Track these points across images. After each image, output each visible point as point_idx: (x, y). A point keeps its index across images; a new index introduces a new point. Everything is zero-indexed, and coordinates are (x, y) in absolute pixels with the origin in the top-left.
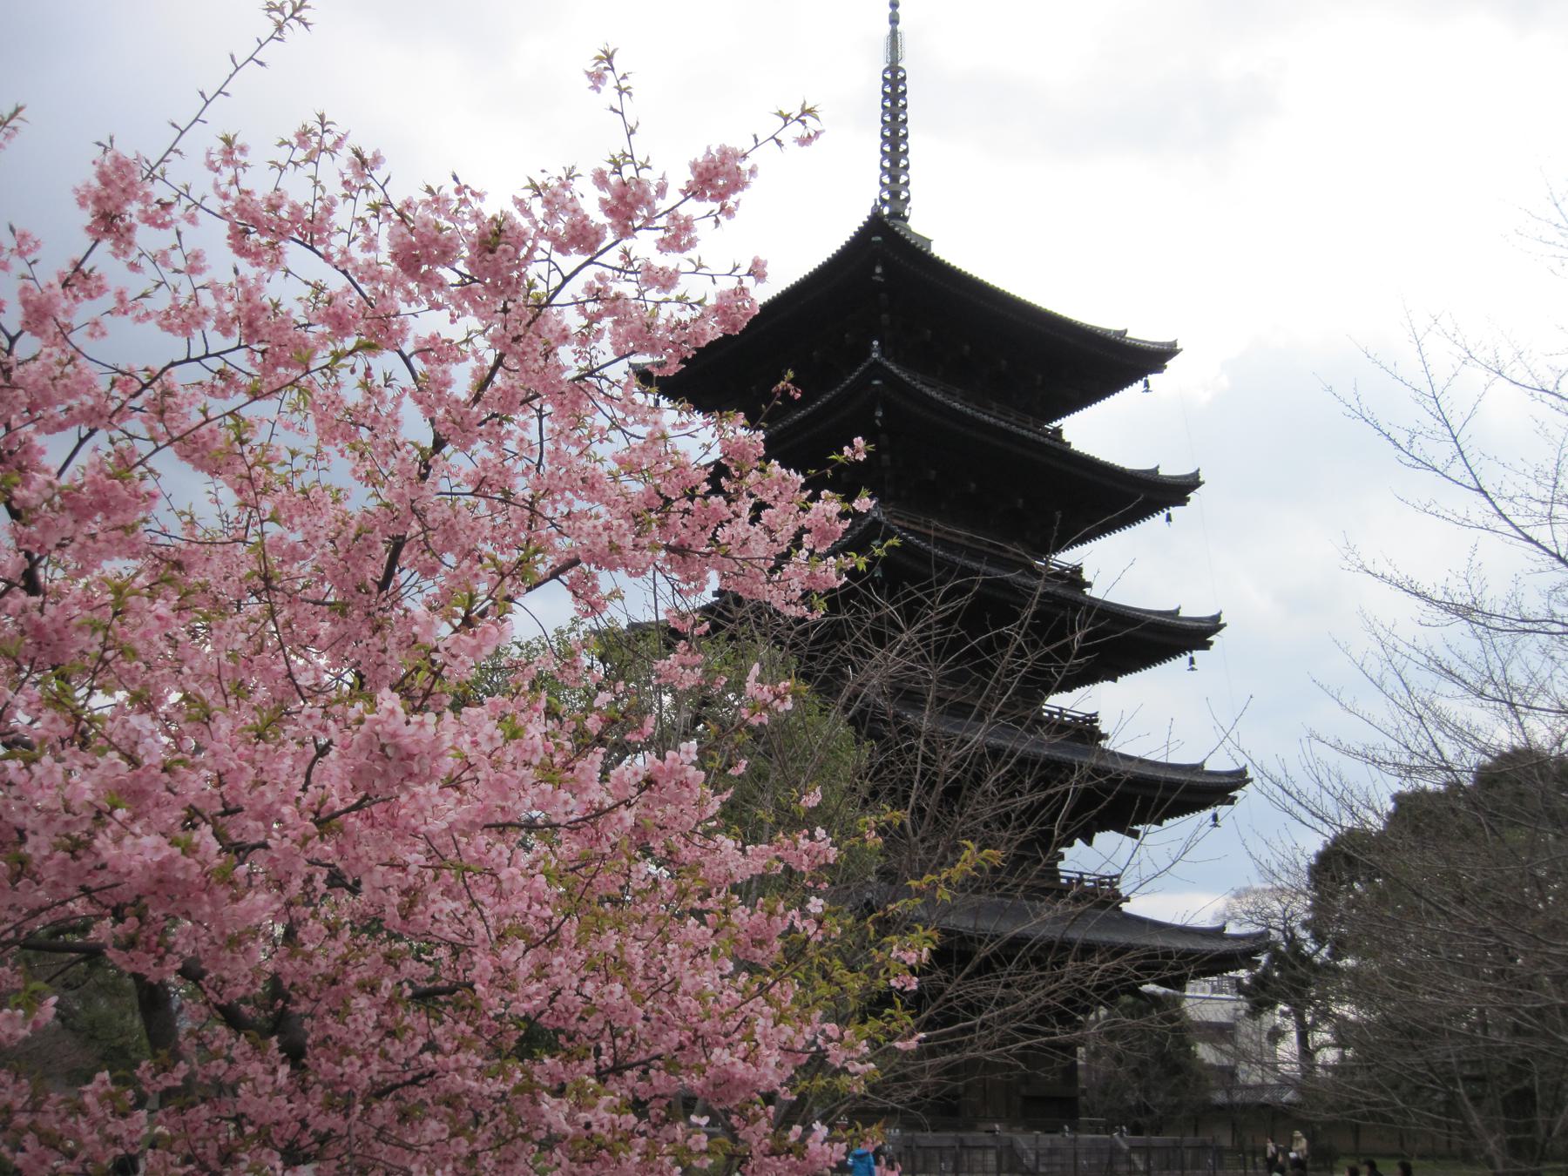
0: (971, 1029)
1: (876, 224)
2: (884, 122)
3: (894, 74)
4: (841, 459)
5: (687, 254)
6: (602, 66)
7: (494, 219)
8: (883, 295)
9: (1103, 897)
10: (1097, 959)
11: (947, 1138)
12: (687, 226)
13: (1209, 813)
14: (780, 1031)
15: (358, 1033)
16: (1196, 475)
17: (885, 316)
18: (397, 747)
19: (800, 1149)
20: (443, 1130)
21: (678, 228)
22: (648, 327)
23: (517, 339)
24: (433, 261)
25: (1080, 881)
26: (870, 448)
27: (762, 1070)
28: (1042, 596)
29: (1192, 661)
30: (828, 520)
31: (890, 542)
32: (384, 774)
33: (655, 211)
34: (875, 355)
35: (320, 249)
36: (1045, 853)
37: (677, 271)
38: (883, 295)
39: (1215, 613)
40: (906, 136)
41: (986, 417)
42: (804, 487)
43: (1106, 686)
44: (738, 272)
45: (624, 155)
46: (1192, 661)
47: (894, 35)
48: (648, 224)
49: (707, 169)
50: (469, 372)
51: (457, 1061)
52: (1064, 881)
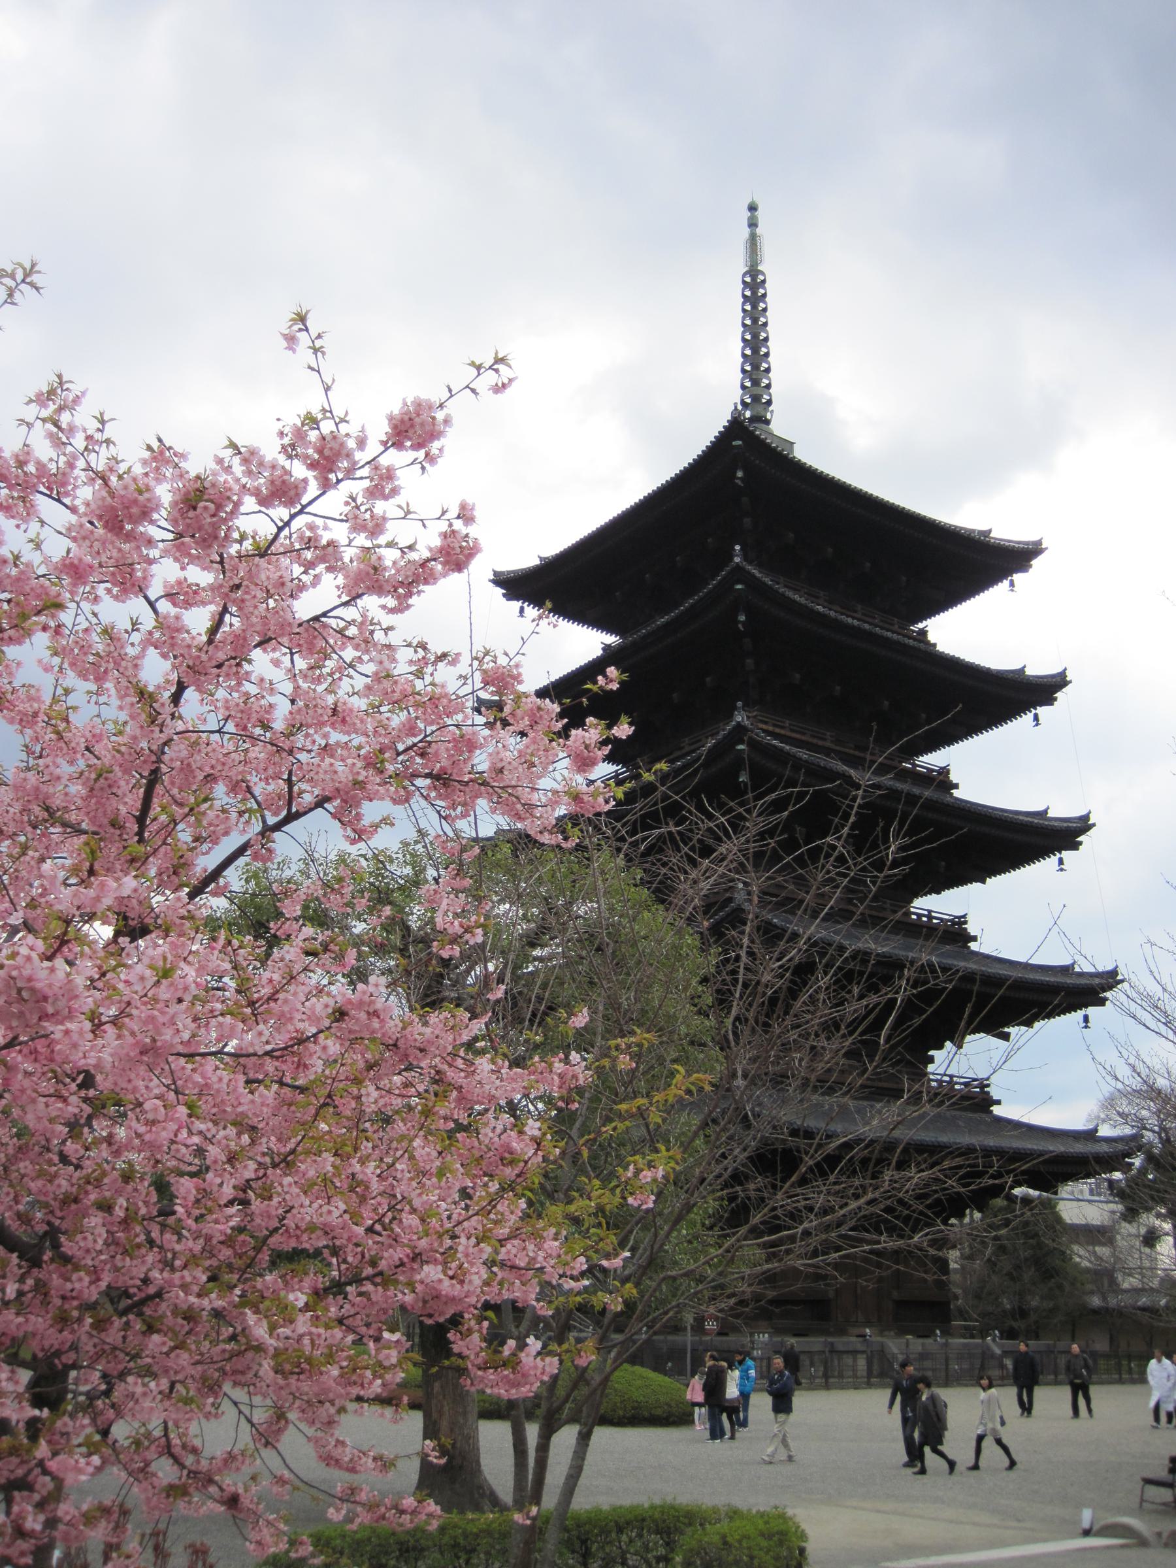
0: (792, 1239)
1: (735, 428)
2: (744, 325)
3: (754, 278)
4: (595, 688)
5: (391, 501)
6: (296, 327)
7: (198, 477)
10: (913, 1170)
11: (815, 1343)
12: (389, 475)
13: (1080, 1014)
14: (481, 1251)
15: (88, 1251)
16: (1063, 674)
18: (33, 990)
19: (513, 1363)
20: (164, 1343)
21: (381, 478)
22: (375, 569)
23: (238, 587)
24: (136, 521)
26: (624, 677)
27: (466, 1287)
28: (860, 806)
29: (1061, 862)
30: (587, 747)
31: (658, 766)
32: (21, 1014)
33: (355, 463)
34: (737, 560)
35: (67, 501)
36: (871, 1062)
37: (384, 519)
38: (745, 500)
39: (1084, 813)
40: (766, 339)
41: (850, 620)
42: (561, 716)
43: (975, 886)
44: (447, 516)
45: (324, 410)
46: (1061, 862)
48: (350, 474)
49: (402, 421)
50: (209, 616)
51: (183, 1277)
52: (934, 1084)
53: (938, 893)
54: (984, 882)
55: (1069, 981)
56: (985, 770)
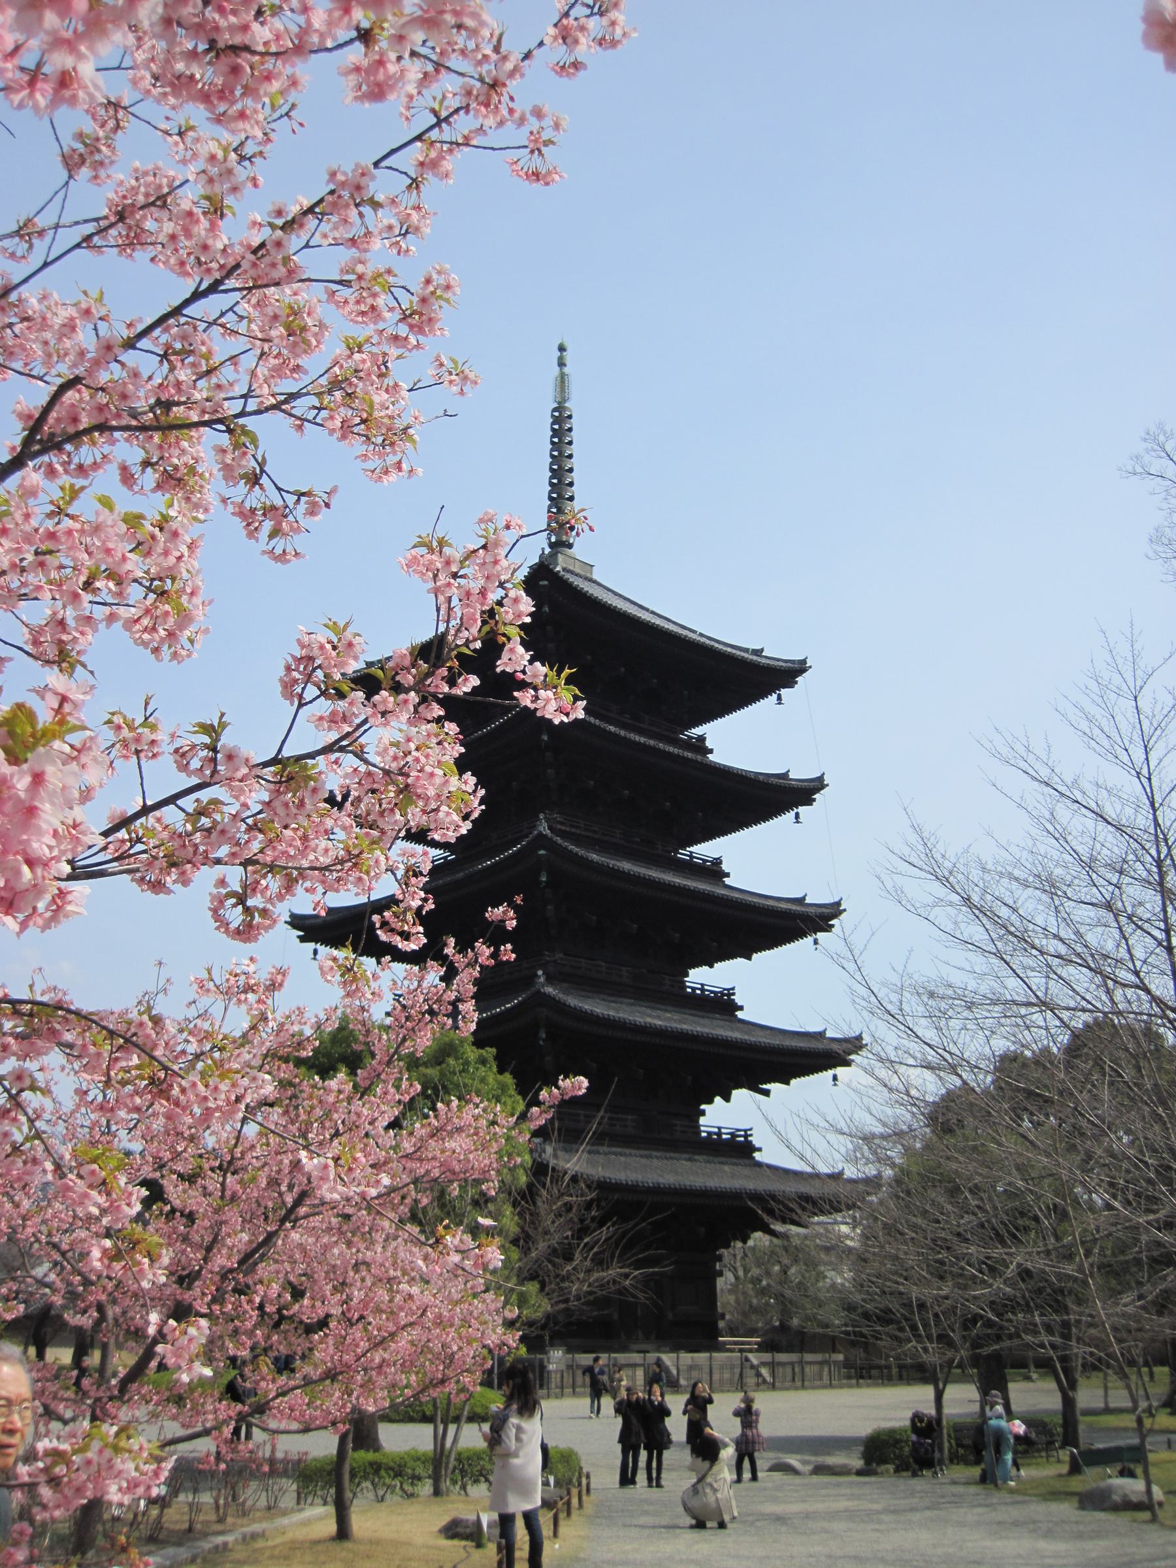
8: (549, 628)
9: (738, 1148)
13: (830, 1072)
16: (820, 779)
17: (551, 646)
25: (719, 1134)
29: (816, 942)
38: (549, 628)
43: (740, 961)
47: (562, 380)
53: (711, 966)
54: (749, 959)
56: (752, 860)
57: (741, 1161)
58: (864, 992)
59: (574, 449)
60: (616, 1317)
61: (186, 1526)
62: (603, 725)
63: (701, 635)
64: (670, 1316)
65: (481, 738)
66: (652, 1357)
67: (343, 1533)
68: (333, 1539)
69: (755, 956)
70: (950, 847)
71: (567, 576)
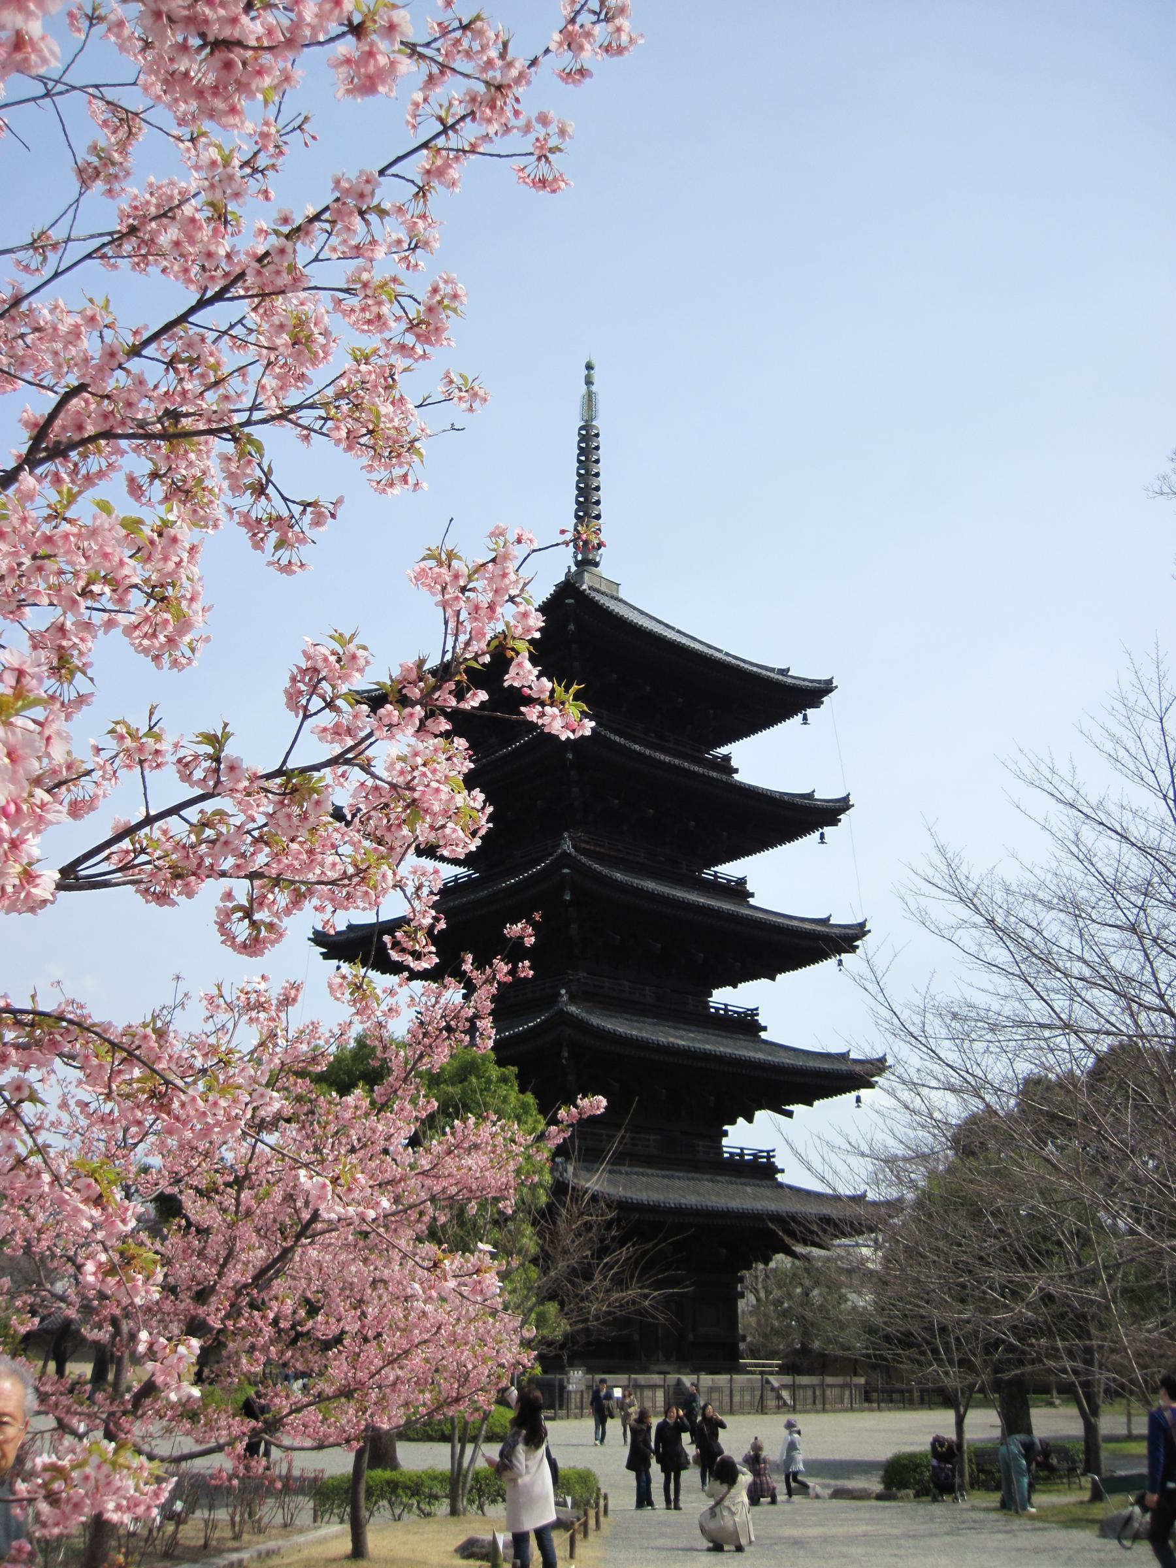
8: (574, 646)
9: (761, 1169)
13: (854, 1094)
17: (576, 664)
25: (742, 1155)
29: (840, 963)
38: (574, 646)
43: (764, 982)
53: (735, 987)
55: (843, 1067)
56: (778, 881)
57: (763, 1183)
58: (887, 1014)
59: (601, 467)
60: (636, 1337)
61: (202, 1542)
62: (628, 744)
63: (727, 654)
64: (691, 1337)
65: (505, 755)
66: (672, 1378)
67: (358, 1551)
68: (348, 1557)
69: (778, 977)
70: (974, 870)
71: (593, 594)
